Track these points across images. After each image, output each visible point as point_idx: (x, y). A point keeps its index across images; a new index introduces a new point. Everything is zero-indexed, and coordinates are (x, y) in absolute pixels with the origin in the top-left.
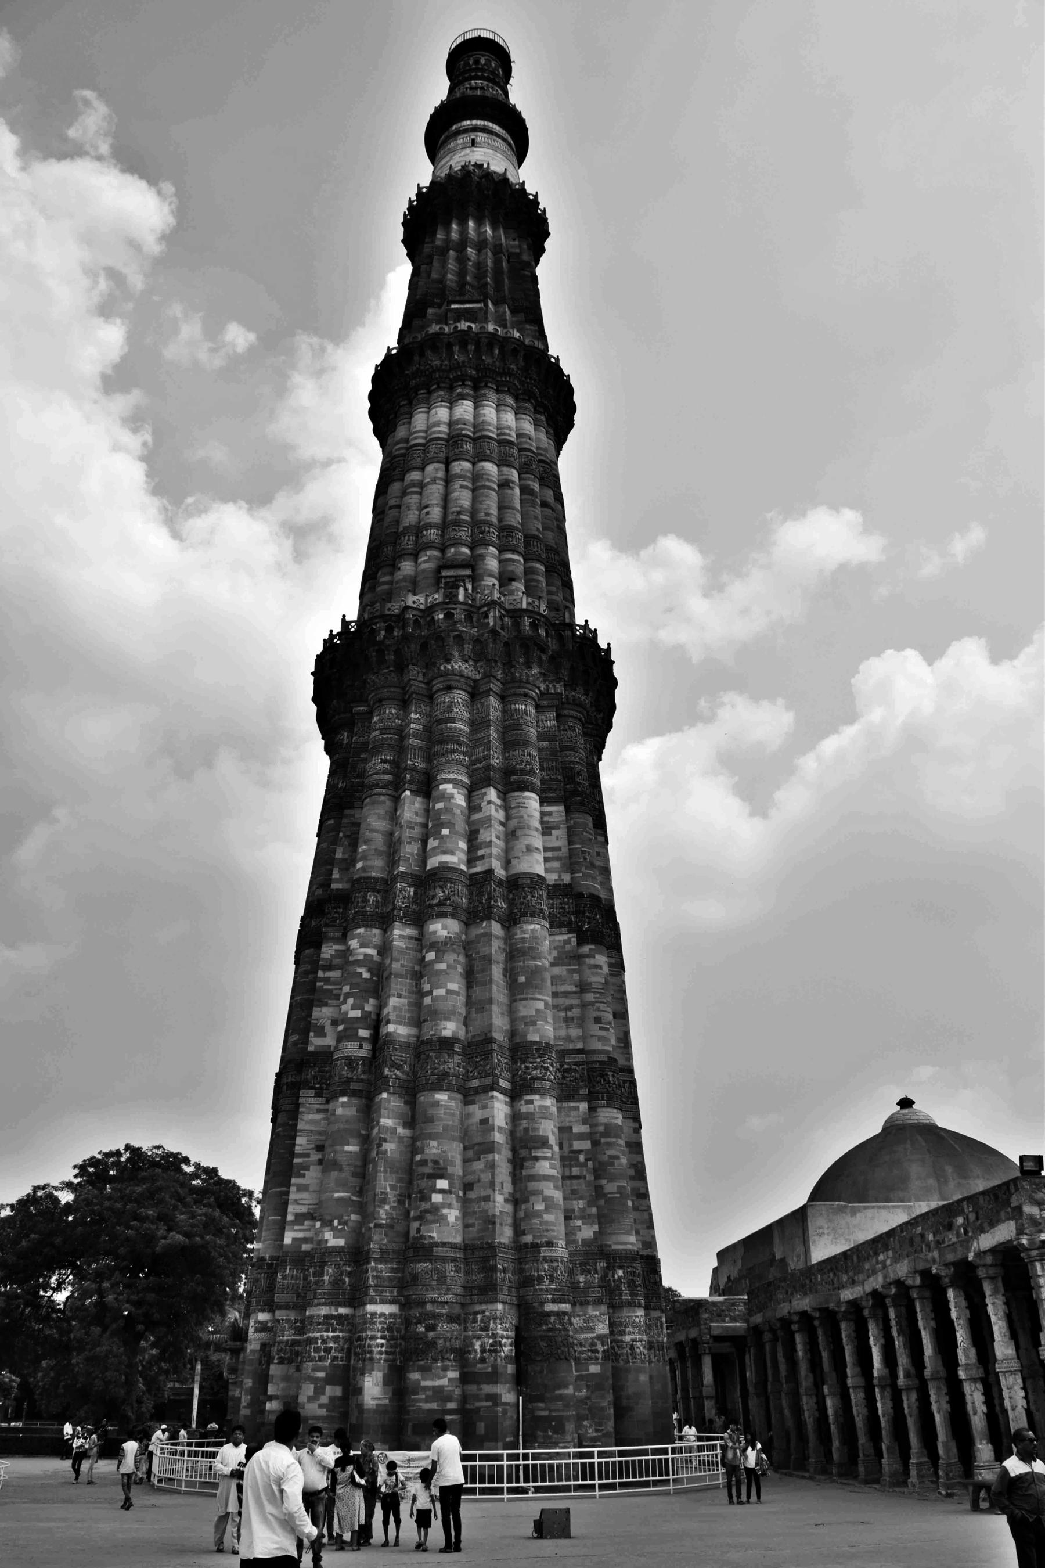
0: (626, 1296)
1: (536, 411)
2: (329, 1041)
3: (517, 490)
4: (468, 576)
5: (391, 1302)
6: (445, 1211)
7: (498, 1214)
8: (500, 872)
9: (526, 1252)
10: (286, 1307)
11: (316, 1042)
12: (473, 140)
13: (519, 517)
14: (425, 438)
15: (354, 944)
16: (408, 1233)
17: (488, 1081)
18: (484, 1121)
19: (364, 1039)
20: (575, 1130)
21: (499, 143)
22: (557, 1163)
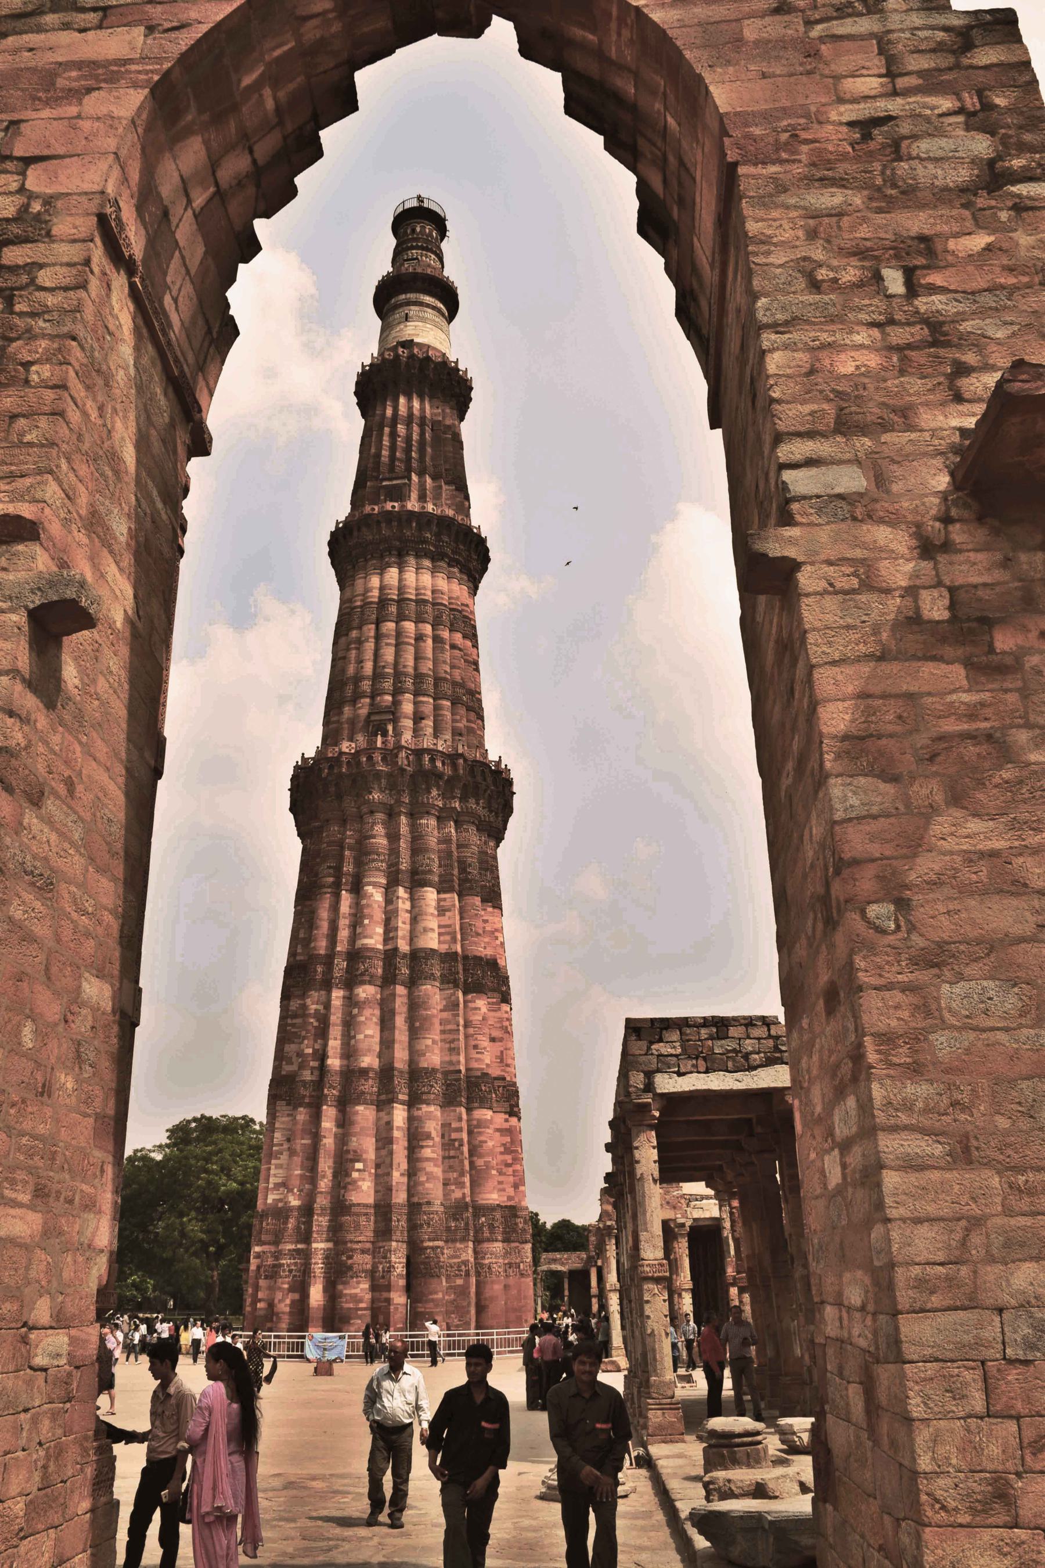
0: (487, 1234)
1: (449, 565)
2: (294, 1068)
3: (430, 642)
5: (327, 1241)
8: (404, 946)
9: (414, 1208)
10: (269, 1243)
11: (287, 1069)
13: (430, 665)
15: (308, 1001)
21: (430, 313)
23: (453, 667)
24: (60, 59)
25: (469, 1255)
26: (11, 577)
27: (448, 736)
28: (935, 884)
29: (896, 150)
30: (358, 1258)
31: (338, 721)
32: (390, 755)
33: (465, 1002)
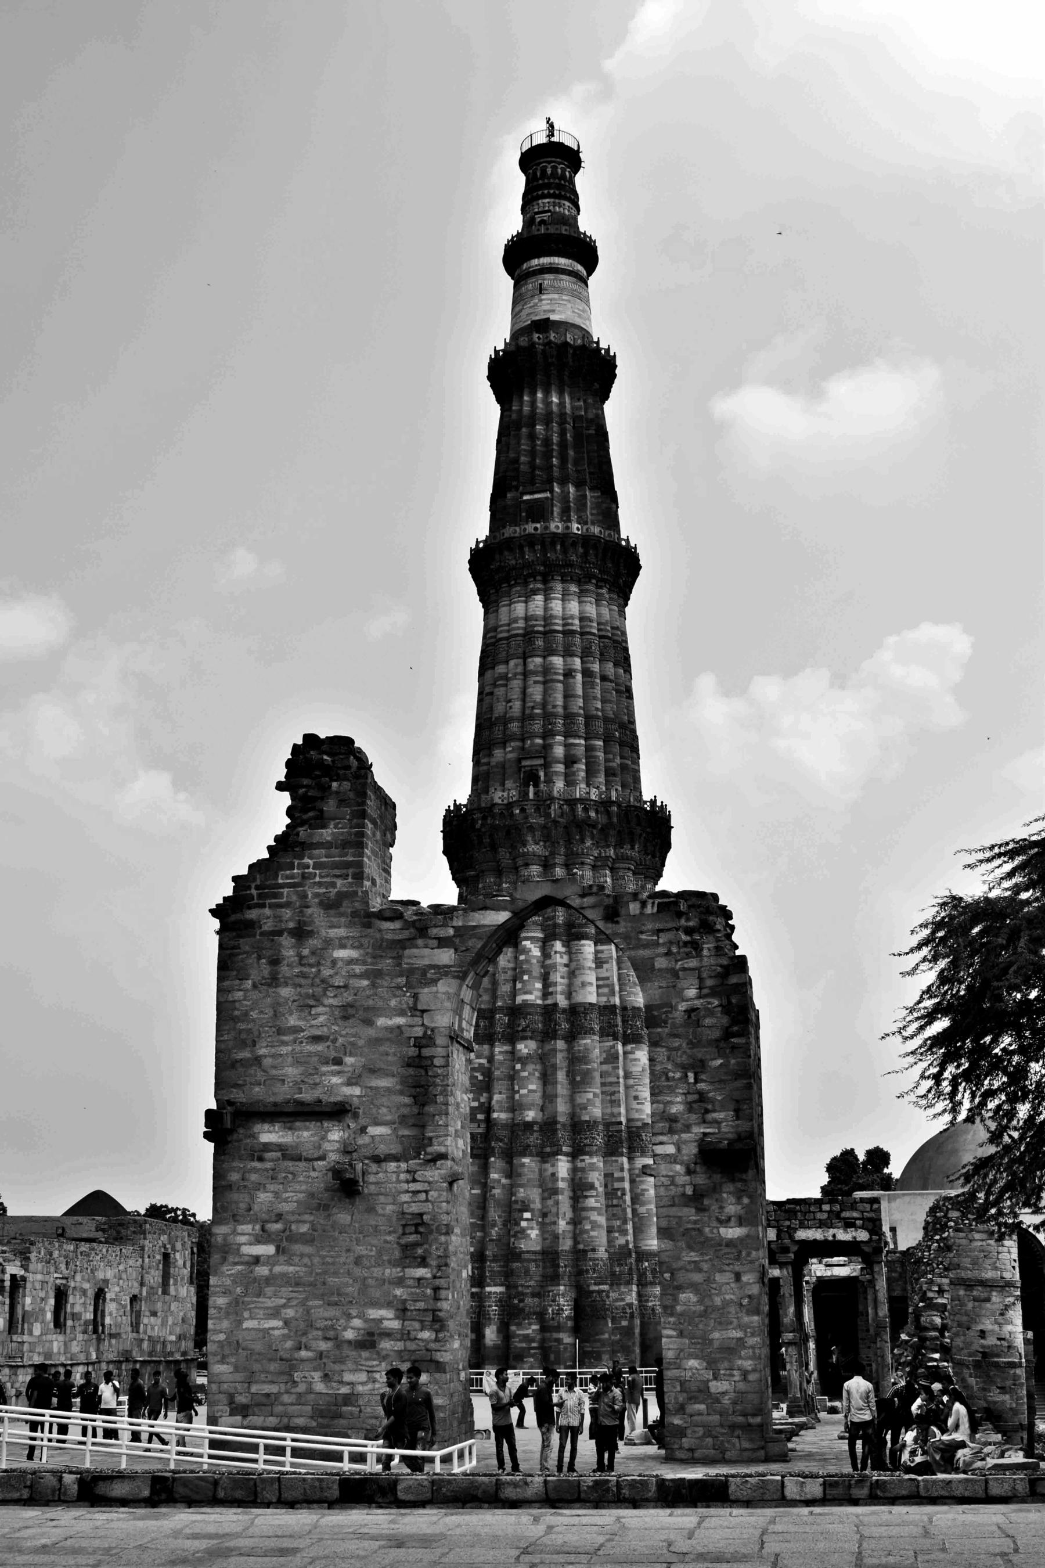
0: (650, 1277)
1: (598, 587)
4: (541, 765)
5: (501, 1285)
6: (529, 1232)
7: (560, 1232)
9: (580, 1254)
12: (541, 284)
14: (508, 631)
16: (509, 1244)
17: (555, 1149)
18: (553, 1174)
19: (481, 1120)
20: (616, 1175)
21: (566, 281)
22: (602, 1200)
23: (603, 702)
24: (427, 963)
25: (632, 1298)
26: (442, 1172)
27: (601, 779)
28: (680, 1269)
29: (698, 1024)
30: (529, 1300)
31: (488, 764)
32: (543, 802)
33: (625, 1053)
